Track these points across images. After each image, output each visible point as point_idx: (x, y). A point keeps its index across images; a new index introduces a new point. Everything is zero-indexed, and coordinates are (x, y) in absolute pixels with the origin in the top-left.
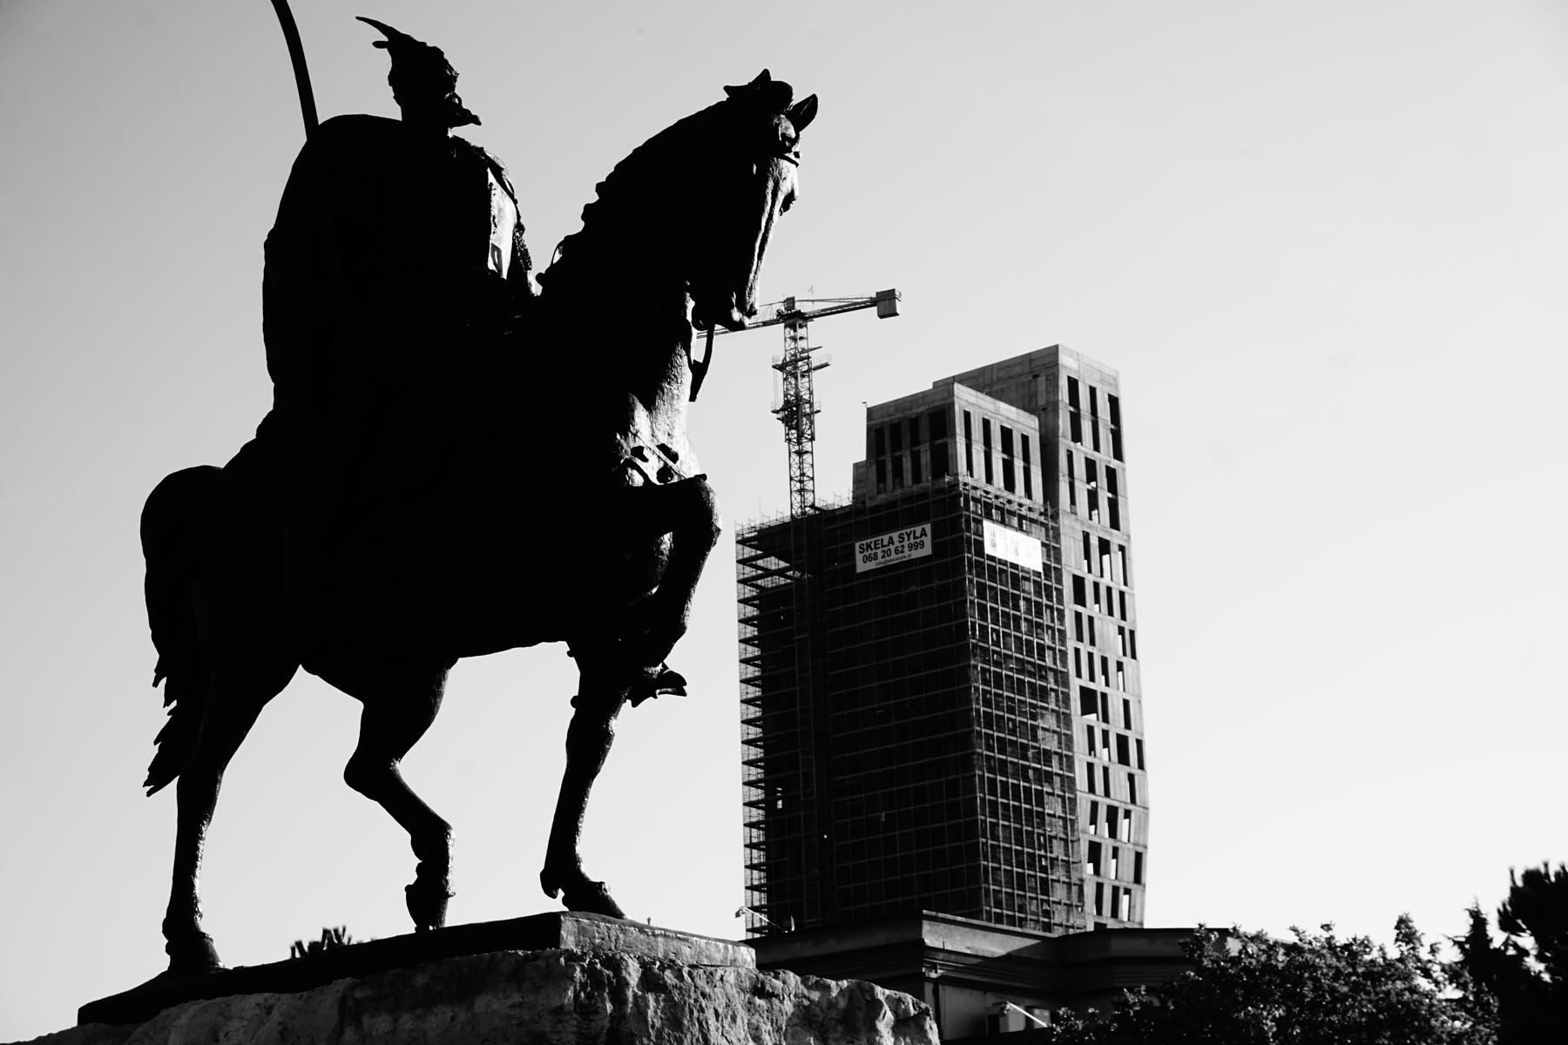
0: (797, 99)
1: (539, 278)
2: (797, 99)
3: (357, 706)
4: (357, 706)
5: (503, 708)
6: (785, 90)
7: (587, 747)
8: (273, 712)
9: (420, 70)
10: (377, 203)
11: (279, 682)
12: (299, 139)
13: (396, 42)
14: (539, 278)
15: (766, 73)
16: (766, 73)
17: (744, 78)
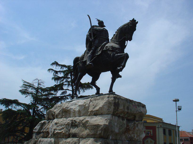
0: (136, 21)
1: (110, 40)
2: (136, 21)
3: (92, 77)
4: (92, 77)
5: (105, 78)
6: (135, 21)
8: (84, 77)
9: (101, 23)
10: (97, 35)
11: (85, 74)
12: (90, 27)
13: (99, 21)
14: (110, 40)
15: (134, 19)
16: (134, 19)
17: (131, 19)
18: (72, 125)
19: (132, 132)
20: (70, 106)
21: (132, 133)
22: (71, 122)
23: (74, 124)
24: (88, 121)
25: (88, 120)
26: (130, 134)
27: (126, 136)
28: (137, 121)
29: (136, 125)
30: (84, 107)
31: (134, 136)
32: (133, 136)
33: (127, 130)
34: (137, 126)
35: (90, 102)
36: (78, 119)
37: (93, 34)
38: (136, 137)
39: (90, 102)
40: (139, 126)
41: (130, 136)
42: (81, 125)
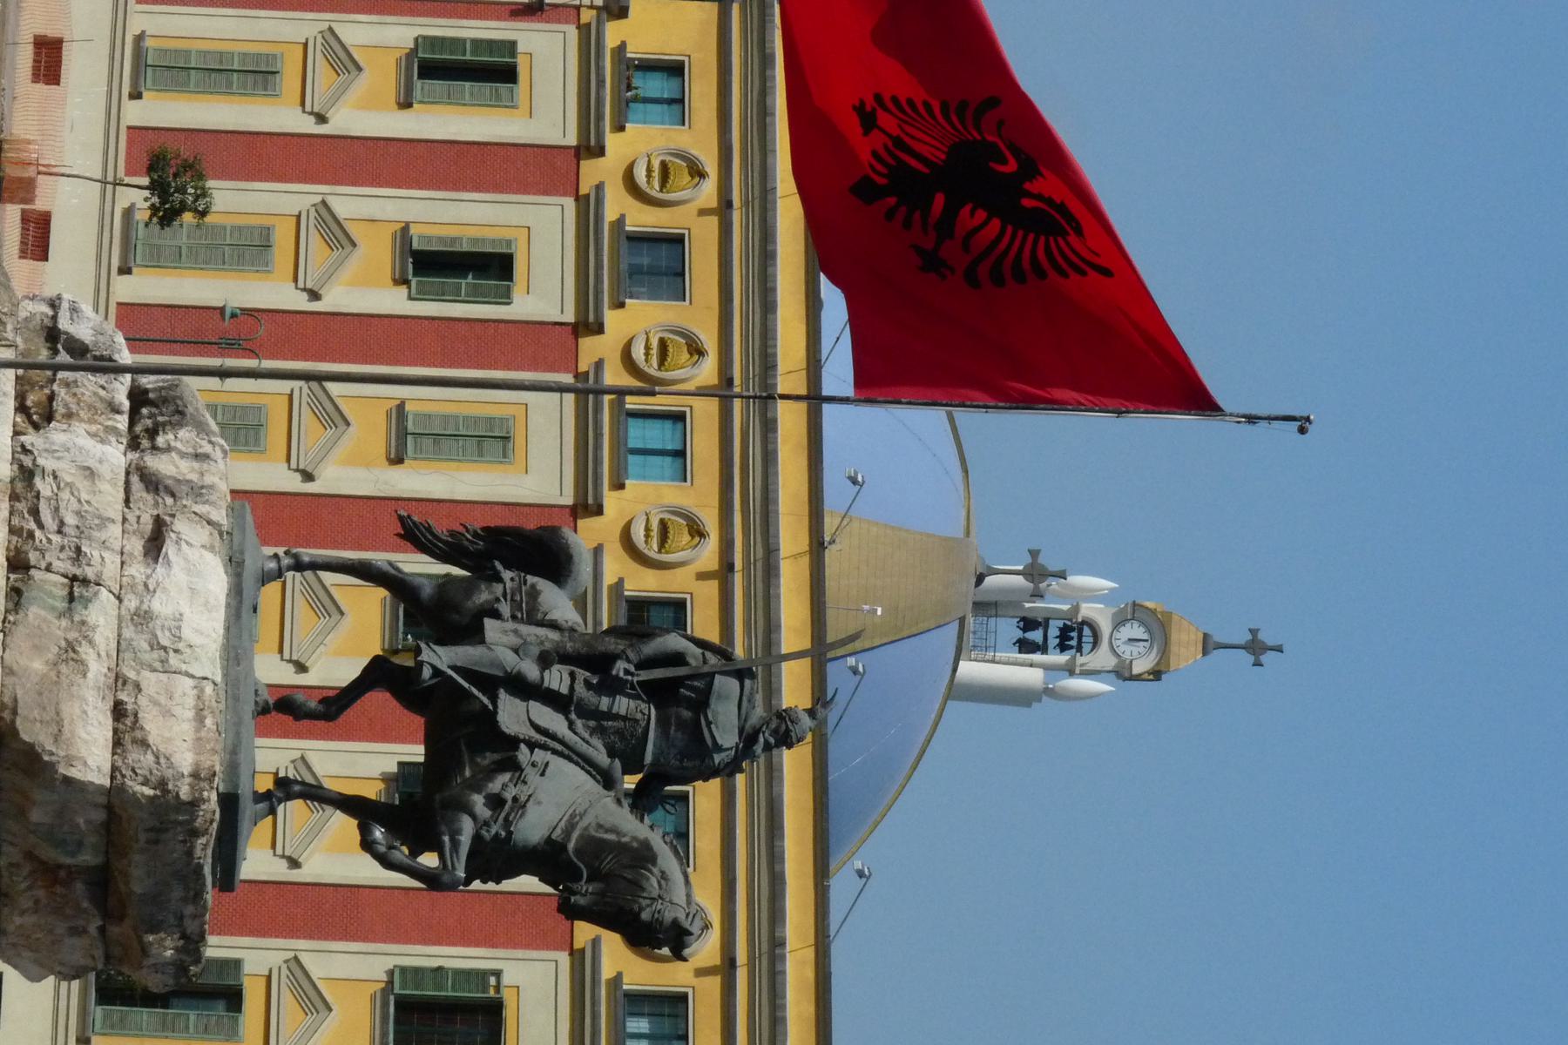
7: (351, 805)
18: (74, 579)
19: (44, 901)
20: (186, 560)
21: (37, 902)
22: (90, 573)
23: (76, 590)
24: (85, 676)
25: (90, 675)
26: (30, 888)
27: (17, 866)
28: (102, 930)
29: (81, 922)
30: (164, 642)
31: (23, 913)
32: (26, 902)
33: (50, 874)
34: (76, 932)
35: (192, 676)
36: (102, 614)
37: (677, 682)
38: (18, 920)
39: (192, 676)
40: (75, 941)
41: (23, 886)
42: (72, 635)
